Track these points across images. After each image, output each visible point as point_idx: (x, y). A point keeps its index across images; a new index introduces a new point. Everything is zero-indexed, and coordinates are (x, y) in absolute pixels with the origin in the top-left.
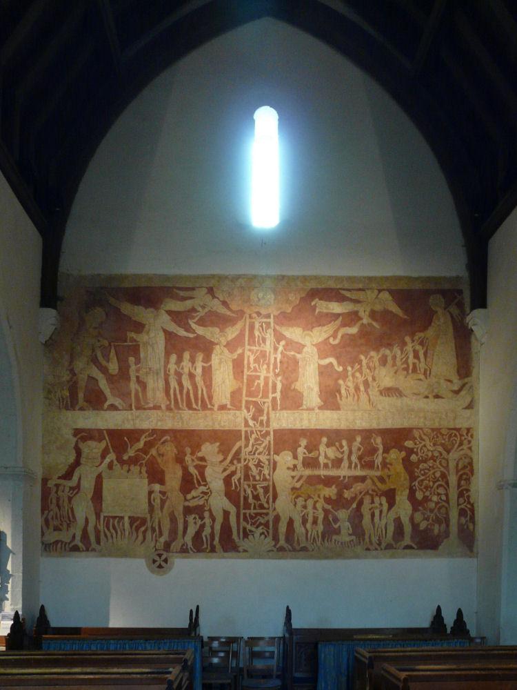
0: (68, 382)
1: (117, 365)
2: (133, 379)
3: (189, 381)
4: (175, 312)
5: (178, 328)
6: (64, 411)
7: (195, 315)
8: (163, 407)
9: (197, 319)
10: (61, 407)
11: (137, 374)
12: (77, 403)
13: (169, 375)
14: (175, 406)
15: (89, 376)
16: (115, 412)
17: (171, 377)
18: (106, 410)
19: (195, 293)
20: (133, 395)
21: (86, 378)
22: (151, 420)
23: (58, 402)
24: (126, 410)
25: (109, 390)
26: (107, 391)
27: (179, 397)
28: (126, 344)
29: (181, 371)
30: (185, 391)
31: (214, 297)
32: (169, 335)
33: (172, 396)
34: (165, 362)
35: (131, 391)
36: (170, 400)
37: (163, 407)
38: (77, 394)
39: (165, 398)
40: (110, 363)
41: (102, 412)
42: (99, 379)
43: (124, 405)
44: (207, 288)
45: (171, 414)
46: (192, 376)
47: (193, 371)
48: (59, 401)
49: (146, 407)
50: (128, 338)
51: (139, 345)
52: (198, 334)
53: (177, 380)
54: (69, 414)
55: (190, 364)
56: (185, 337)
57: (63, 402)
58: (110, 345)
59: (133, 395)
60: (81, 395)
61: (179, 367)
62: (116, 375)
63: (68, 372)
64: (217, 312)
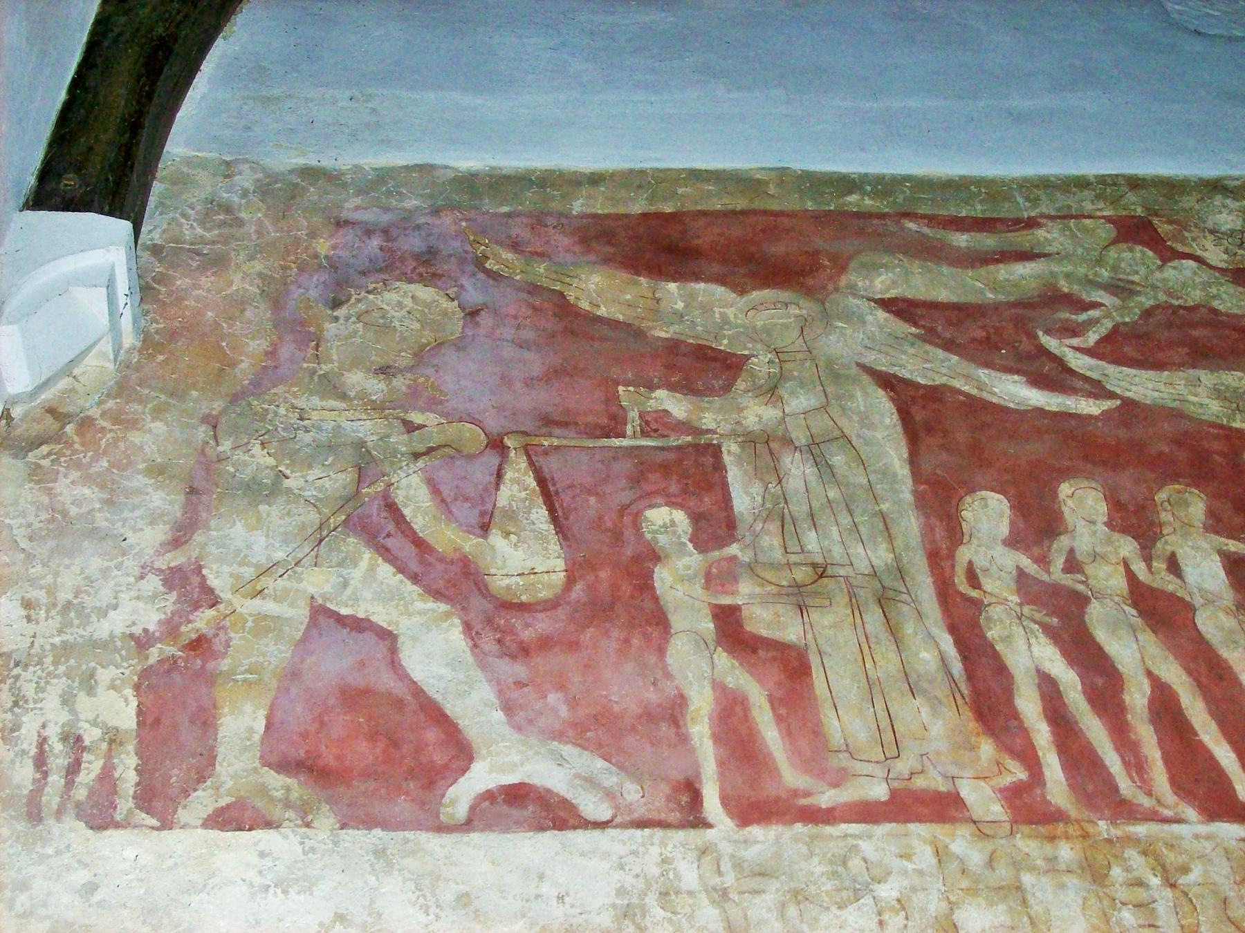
0: (142, 642)
1: (554, 546)
2: (690, 616)
3: (1148, 639)
4: (933, 306)
5: (983, 374)
6: (73, 831)
7: (1083, 317)
8: (982, 799)
9: (1092, 338)
10: (51, 798)
11: (726, 600)
12: (203, 771)
13: (977, 605)
14: (1074, 786)
15: (321, 614)
16: (550, 839)
17: (996, 612)
18: (467, 825)
19: (1049, 236)
20: (701, 731)
21: (301, 613)
22: (888, 891)
23: (24, 774)
24: (641, 824)
25: (484, 692)
26: (473, 702)
27: (1095, 730)
28: (617, 442)
29: (1068, 580)
30: (1137, 697)
31: (1168, 255)
32: (920, 410)
33: (1042, 734)
34: (928, 530)
35: (681, 701)
36: (1030, 759)
37: (982, 799)
38: (206, 721)
39: (987, 748)
40: (496, 538)
41: (433, 843)
42: (404, 626)
43: (632, 792)
44: (1108, 219)
45: (1066, 852)
46: (1162, 612)
47: (1164, 581)
48: (40, 761)
49: (827, 798)
50: (633, 414)
51: (716, 451)
52: (1129, 405)
53: (1047, 629)
54: (129, 852)
55: (1127, 547)
56: (1040, 412)
57: (73, 769)
58: (497, 445)
59: (701, 731)
60: (241, 725)
61: (1043, 561)
62: (551, 605)
63: (153, 583)
64: (1215, 311)
